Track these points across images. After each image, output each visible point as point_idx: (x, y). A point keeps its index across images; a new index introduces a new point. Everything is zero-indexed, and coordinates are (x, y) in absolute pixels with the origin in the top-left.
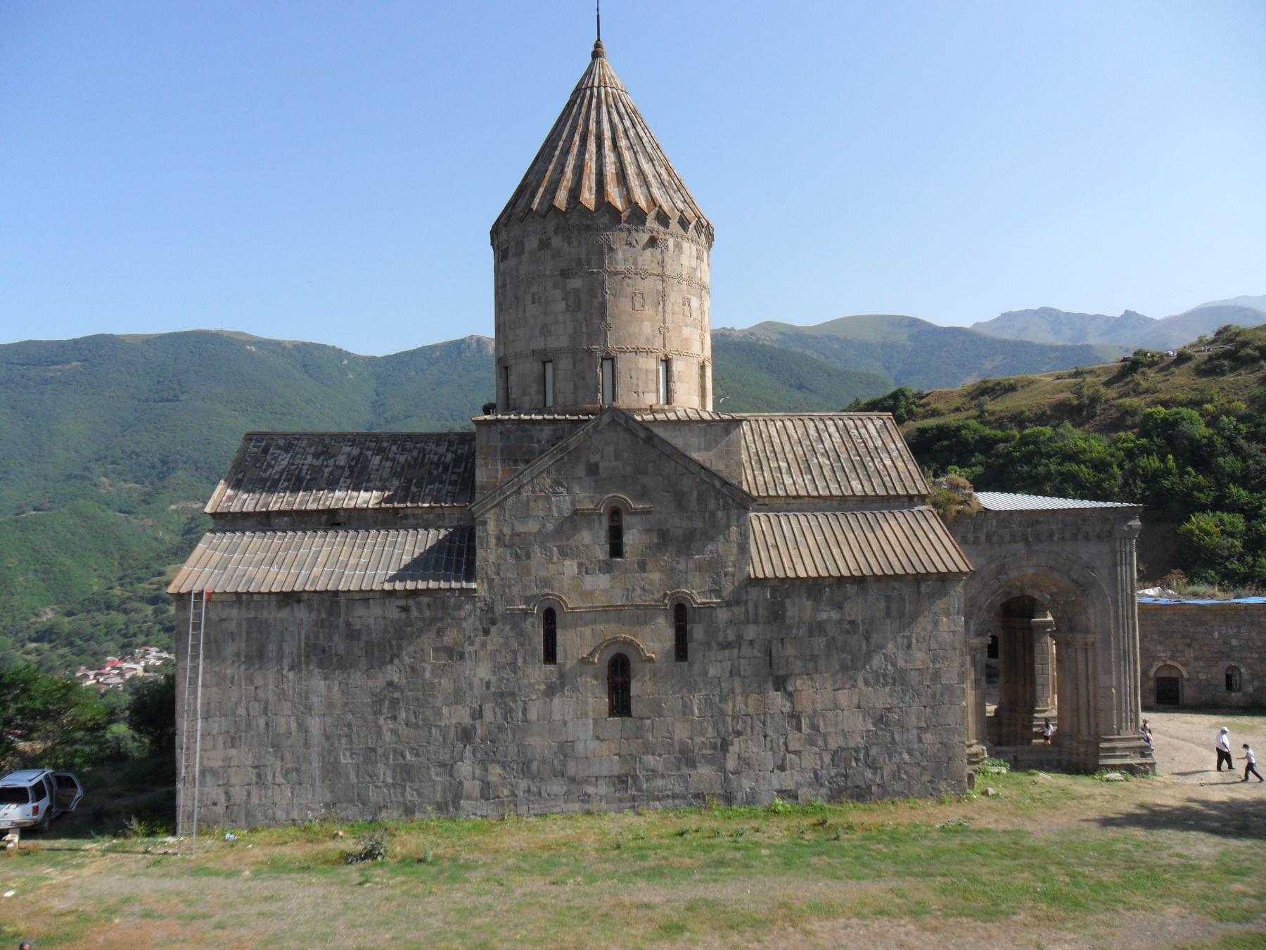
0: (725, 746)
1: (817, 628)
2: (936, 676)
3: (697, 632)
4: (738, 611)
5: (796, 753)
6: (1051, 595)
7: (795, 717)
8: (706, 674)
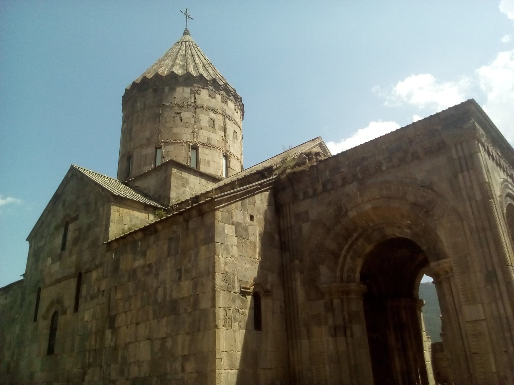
0: (84, 374)
1: (133, 274)
2: (196, 304)
3: (84, 291)
4: (100, 270)
6: (409, 227)
7: (115, 349)
8: (83, 318)
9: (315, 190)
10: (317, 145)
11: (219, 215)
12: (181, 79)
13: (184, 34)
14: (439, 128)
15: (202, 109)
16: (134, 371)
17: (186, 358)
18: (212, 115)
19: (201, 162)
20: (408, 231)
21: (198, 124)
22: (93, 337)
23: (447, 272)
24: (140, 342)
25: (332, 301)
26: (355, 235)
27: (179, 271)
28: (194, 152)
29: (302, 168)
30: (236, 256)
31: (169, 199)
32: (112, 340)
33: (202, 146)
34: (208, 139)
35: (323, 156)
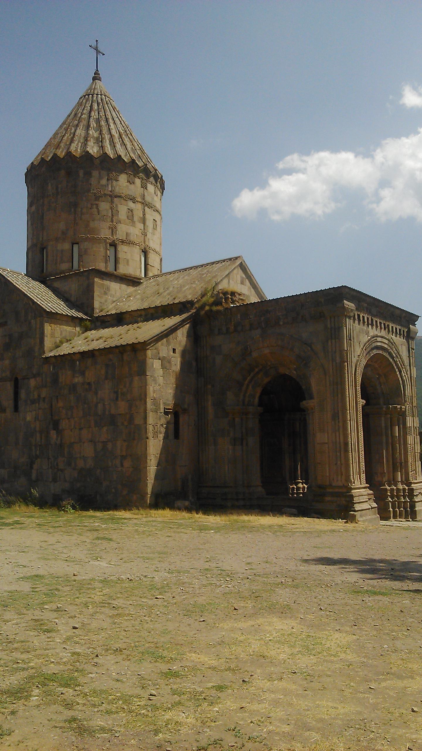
0: (32, 463)
1: (73, 388)
2: (131, 420)
3: (23, 395)
5: (62, 470)
6: (295, 370)
8: (25, 419)
9: (228, 329)
10: (237, 266)
11: (149, 353)
12: (97, 162)
13: (94, 79)
14: (322, 300)
15: (120, 199)
16: (81, 464)
17: (123, 458)
18: (131, 204)
19: (120, 262)
20: (295, 372)
21: (116, 217)
22: (38, 435)
23: (312, 409)
24: (83, 443)
25: (234, 419)
26: (257, 370)
27: (116, 393)
28: (113, 249)
29: (219, 308)
30: (162, 384)
31: (93, 309)
32: (57, 439)
33: (121, 243)
34: (127, 234)
35: (237, 296)
